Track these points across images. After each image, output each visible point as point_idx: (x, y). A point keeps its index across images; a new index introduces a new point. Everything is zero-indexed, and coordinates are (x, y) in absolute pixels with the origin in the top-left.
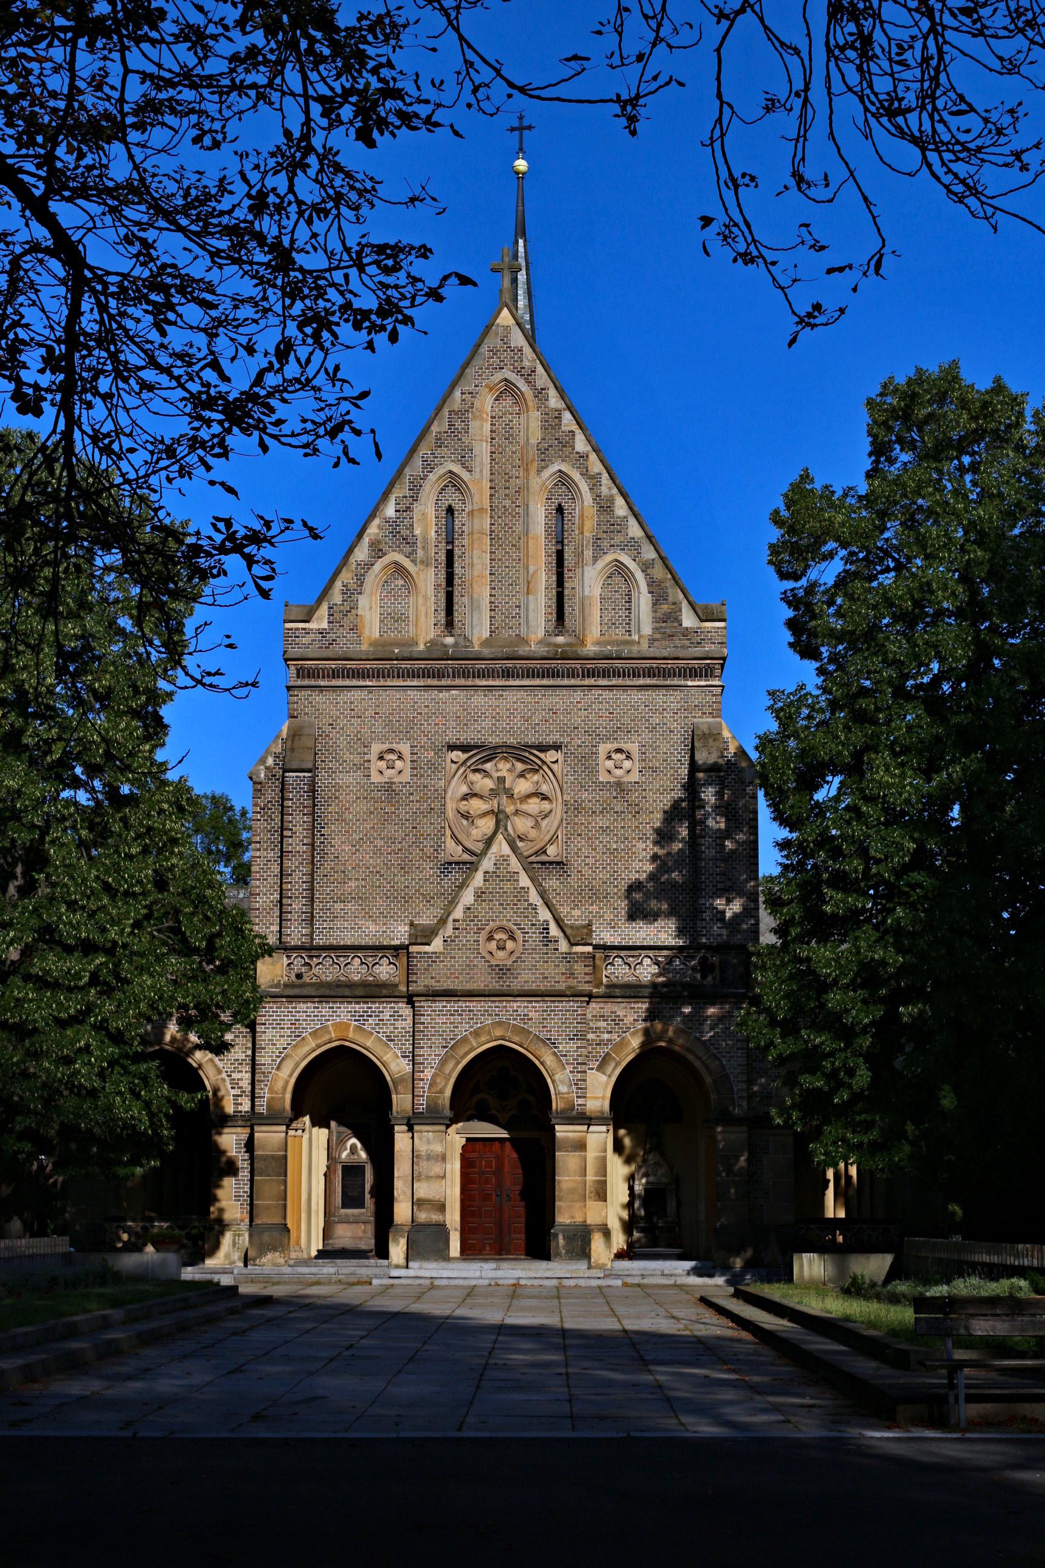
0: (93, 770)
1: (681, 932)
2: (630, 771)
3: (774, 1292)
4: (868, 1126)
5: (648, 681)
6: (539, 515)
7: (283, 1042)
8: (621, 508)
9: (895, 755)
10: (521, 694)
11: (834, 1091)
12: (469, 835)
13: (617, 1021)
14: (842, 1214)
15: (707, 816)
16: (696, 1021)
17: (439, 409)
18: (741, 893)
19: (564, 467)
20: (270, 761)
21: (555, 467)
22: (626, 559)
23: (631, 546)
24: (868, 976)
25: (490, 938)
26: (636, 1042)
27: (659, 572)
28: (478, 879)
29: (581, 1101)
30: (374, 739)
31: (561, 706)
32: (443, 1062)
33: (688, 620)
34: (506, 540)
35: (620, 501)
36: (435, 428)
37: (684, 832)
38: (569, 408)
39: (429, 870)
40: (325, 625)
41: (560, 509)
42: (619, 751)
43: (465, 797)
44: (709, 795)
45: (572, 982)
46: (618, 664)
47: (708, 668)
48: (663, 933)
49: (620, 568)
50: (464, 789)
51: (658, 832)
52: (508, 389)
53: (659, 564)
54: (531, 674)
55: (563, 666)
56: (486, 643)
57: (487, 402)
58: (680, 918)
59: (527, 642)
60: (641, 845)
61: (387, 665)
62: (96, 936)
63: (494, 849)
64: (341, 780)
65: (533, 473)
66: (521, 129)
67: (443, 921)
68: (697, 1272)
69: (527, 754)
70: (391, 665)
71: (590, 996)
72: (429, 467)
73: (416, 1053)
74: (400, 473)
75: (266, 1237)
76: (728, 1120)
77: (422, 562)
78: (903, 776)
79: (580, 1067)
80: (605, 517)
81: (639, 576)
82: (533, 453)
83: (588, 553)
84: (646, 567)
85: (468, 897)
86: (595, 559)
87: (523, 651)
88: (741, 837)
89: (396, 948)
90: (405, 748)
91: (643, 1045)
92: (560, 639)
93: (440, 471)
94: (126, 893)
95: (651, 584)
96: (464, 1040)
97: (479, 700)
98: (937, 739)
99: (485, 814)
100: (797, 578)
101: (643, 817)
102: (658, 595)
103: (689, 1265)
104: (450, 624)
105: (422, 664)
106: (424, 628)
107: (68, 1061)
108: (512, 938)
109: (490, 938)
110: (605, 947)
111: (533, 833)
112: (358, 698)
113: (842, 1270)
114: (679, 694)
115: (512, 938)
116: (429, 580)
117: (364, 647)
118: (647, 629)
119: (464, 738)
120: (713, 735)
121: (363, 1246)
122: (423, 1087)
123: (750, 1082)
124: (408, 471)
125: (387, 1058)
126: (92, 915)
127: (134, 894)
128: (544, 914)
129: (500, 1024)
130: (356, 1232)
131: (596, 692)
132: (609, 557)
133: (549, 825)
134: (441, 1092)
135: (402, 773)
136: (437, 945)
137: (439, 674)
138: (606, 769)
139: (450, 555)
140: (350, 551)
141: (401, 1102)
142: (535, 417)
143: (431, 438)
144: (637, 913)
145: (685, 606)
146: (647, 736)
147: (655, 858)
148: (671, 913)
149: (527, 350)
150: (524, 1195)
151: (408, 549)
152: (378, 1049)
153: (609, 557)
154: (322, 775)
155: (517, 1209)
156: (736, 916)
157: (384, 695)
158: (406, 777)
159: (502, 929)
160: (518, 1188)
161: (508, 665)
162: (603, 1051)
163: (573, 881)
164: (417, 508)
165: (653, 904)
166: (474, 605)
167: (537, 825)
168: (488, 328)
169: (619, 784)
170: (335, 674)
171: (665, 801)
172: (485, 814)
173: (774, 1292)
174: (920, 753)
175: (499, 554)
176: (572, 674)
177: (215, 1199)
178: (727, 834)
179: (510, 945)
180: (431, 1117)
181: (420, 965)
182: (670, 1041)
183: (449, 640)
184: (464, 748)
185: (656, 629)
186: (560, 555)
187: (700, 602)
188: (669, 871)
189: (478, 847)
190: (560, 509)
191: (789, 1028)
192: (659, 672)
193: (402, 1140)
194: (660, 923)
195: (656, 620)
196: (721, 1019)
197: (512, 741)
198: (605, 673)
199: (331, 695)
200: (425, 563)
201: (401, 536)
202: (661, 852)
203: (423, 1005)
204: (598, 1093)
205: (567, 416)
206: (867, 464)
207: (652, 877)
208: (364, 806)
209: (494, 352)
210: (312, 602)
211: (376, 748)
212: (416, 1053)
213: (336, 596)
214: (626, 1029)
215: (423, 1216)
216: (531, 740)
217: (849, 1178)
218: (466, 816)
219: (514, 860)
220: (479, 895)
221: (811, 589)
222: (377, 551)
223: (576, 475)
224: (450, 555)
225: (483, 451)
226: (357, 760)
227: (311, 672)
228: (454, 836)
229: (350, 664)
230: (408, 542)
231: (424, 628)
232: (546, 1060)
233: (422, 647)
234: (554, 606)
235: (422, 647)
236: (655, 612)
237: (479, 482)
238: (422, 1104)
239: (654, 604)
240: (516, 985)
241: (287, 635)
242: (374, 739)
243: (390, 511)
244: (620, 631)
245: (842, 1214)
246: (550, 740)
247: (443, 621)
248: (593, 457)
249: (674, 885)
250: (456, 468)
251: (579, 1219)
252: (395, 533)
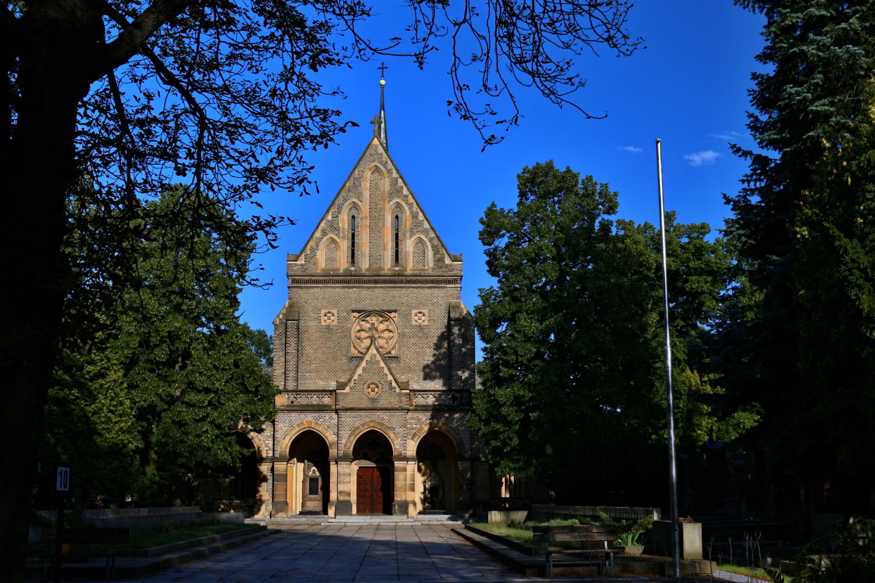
0: (210, 320)
1: (444, 385)
2: (424, 321)
3: (480, 526)
4: (518, 460)
5: (432, 285)
6: (389, 219)
7: (285, 429)
8: (421, 217)
9: (528, 314)
10: (381, 290)
11: (504, 447)
13: (419, 420)
14: (508, 496)
15: (455, 338)
16: (450, 420)
17: (349, 177)
18: (468, 369)
19: (398, 200)
20: (281, 316)
21: (395, 200)
22: (423, 237)
23: (425, 232)
24: (518, 401)
25: (369, 387)
26: (426, 428)
27: (436, 242)
28: (364, 364)
30: (324, 309)
31: (397, 295)
32: (350, 436)
33: (448, 261)
34: (376, 228)
35: (421, 214)
36: (347, 185)
37: (446, 345)
38: (401, 177)
39: (344, 360)
40: (303, 262)
41: (397, 217)
42: (420, 313)
43: (359, 331)
44: (456, 330)
45: (401, 405)
46: (419, 278)
47: (456, 280)
48: (437, 385)
49: (420, 240)
50: (358, 328)
51: (435, 344)
52: (377, 169)
53: (436, 239)
54: (385, 282)
55: (398, 279)
56: (367, 270)
57: (368, 175)
58: (445, 379)
59: (384, 270)
60: (428, 350)
61: (328, 278)
62: (210, 386)
63: (370, 351)
64: (309, 324)
65: (386, 202)
66: (383, 68)
67: (350, 380)
68: (450, 519)
69: (383, 314)
70: (330, 278)
71: (408, 410)
72: (345, 200)
73: (339, 433)
74: (334, 202)
75: (279, 507)
76: (463, 459)
78: (531, 323)
79: (404, 438)
81: (428, 244)
82: (386, 195)
83: (408, 235)
84: (431, 240)
85: (360, 371)
86: (411, 237)
87: (382, 273)
88: (468, 347)
89: (331, 391)
90: (335, 311)
91: (429, 429)
92: (397, 268)
93: (350, 201)
94: (223, 369)
95: (434, 247)
96: (358, 427)
97: (365, 292)
98: (545, 308)
99: (366, 338)
100: (490, 244)
101: (430, 339)
102: (436, 251)
103: (447, 516)
104: (353, 262)
105: (342, 278)
106: (343, 263)
107: (199, 436)
108: (377, 387)
109: (369, 387)
110: (414, 391)
111: (386, 346)
112: (317, 292)
113: (508, 517)
114: (444, 290)
115: (377, 387)
116: (344, 245)
117: (319, 271)
118: (431, 264)
119: (358, 307)
120: (457, 306)
121: (318, 510)
122: (342, 446)
123: (472, 444)
124: (337, 202)
125: (327, 435)
126: (209, 377)
127: (226, 370)
128: (390, 378)
129: (372, 421)
130: (315, 504)
131: (411, 289)
132: (416, 236)
133: (392, 342)
135: (333, 321)
136: (347, 390)
137: (349, 282)
138: (416, 320)
139: (353, 235)
140: (314, 233)
141: (333, 452)
142: (387, 182)
143: (346, 189)
144: (427, 377)
145: (446, 256)
146: (431, 307)
147: (434, 355)
148: (440, 377)
149: (384, 154)
150: (382, 489)
152: (324, 431)
153: (416, 236)
154: (302, 322)
155: (379, 494)
156: (466, 378)
157: (326, 290)
158: (335, 323)
159: (373, 383)
160: (379, 487)
161: (376, 279)
163: (402, 364)
164: (340, 216)
165: (434, 373)
166: (363, 255)
167: (387, 342)
168: (369, 145)
169: (420, 326)
170: (307, 282)
171: (438, 333)
172: (366, 338)
173: (480, 526)
174: (538, 314)
175: (373, 235)
176: (401, 282)
177: (259, 491)
178: (463, 346)
179: (376, 390)
180: (344, 458)
181: (340, 397)
182: (440, 428)
183: (353, 269)
184: (359, 312)
186: (397, 235)
187: (452, 253)
188: (440, 360)
189: (364, 351)
190: (397, 217)
191: (487, 422)
192: (436, 281)
193: (333, 468)
194: (436, 381)
195: (435, 261)
196: (460, 419)
197: (378, 309)
198: (414, 282)
199: (305, 290)
200: (343, 238)
201: (334, 227)
202: (437, 353)
203: (342, 413)
204: (412, 448)
205: (400, 180)
206: (518, 200)
207: (433, 362)
208: (318, 335)
209: (371, 155)
210: (298, 253)
211: (323, 311)
212: (339, 433)
213: (308, 251)
214: (422, 423)
215: (341, 498)
216: (385, 308)
217: (511, 481)
218: (359, 338)
219: (378, 356)
220: (364, 370)
221: (496, 249)
222: (324, 233)
223: (403, 204)
224: (353, 235)
225: (366, 194)
226: (316, 316)
227: (298, 281)
228: (354, 346)
229: (313, 278)
230: (336, 229)
231: (343, 263)
232: (391, 436)
235: (342, 271)
237: (365, 206)
238: (341, 453)
239: (434, 255)
240: (379, 406)
241: (289, 266)
242: (324, 309)
243: (329, 217)
244: (421, 265)
245: (508, 496)
246: (393, 308)
248: (410, 196)
249: (442, 366)
250: (356, 201)
251: (404, 499)
252: (331, 226)
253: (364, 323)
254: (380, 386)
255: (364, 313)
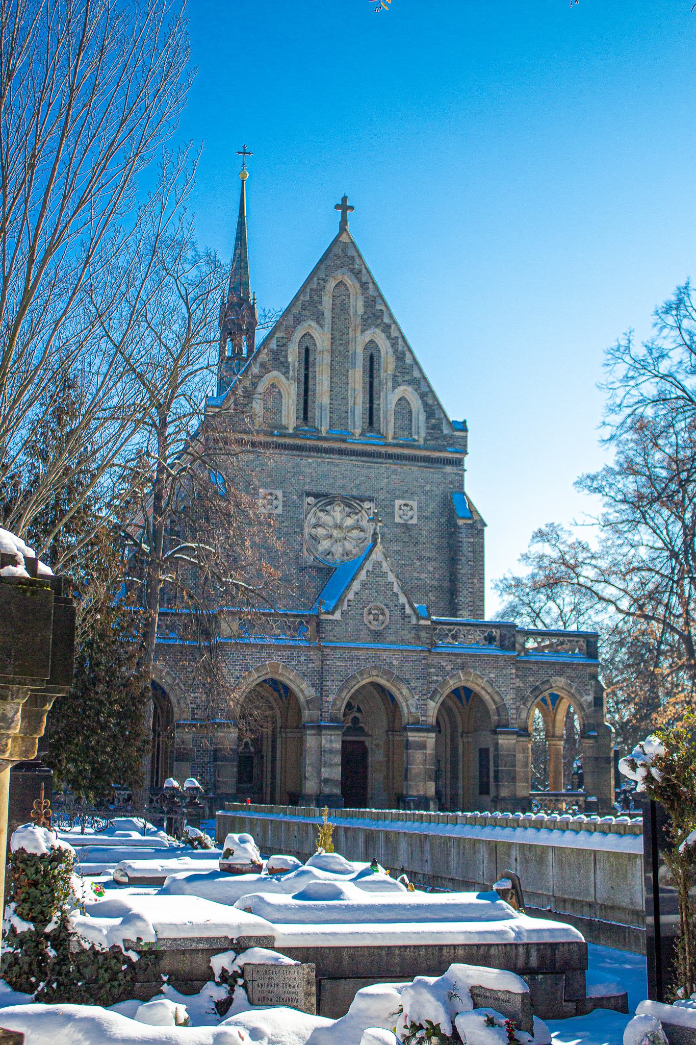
12: (317, 550)
13: (441, 668)
25: (370, 613)
29: (423, 718)
32: (341, 691)
34: (338, 372)
41: (372, 357)
42: (406, 505)
50: (313, 521)
63: (373, 556)
69: (352, 502)
77: (292, 379)
80: (400, 363)
85: (356, 586)
86: (394, 388)
96: (354, 677)
104: (306, 418)
108: (383, 614)
109: (370, 613)
115: (383, 614)
118: (423, 434)
119: (314, 490)
128: (403, 599)
134: (339, 710)
136: (337, 616)
151: (284, 370)
159: (377, 608)
162: (433, 687)
175: (335, 380)
179: (381, 617)
181: (328, 628)
184: (316, 496)
185: (428, 433)
190: (372, 357)
195: (427, 428)
220: (364, 584)
233: (291, 431)
234: (368, 414)
235: (291, 431)
236: (427, 423)
239: (427, 419)
246: (367, 494)
247: (302, 416)
253: (321, 514)
254: (387, 612)
255: (325, 499)
